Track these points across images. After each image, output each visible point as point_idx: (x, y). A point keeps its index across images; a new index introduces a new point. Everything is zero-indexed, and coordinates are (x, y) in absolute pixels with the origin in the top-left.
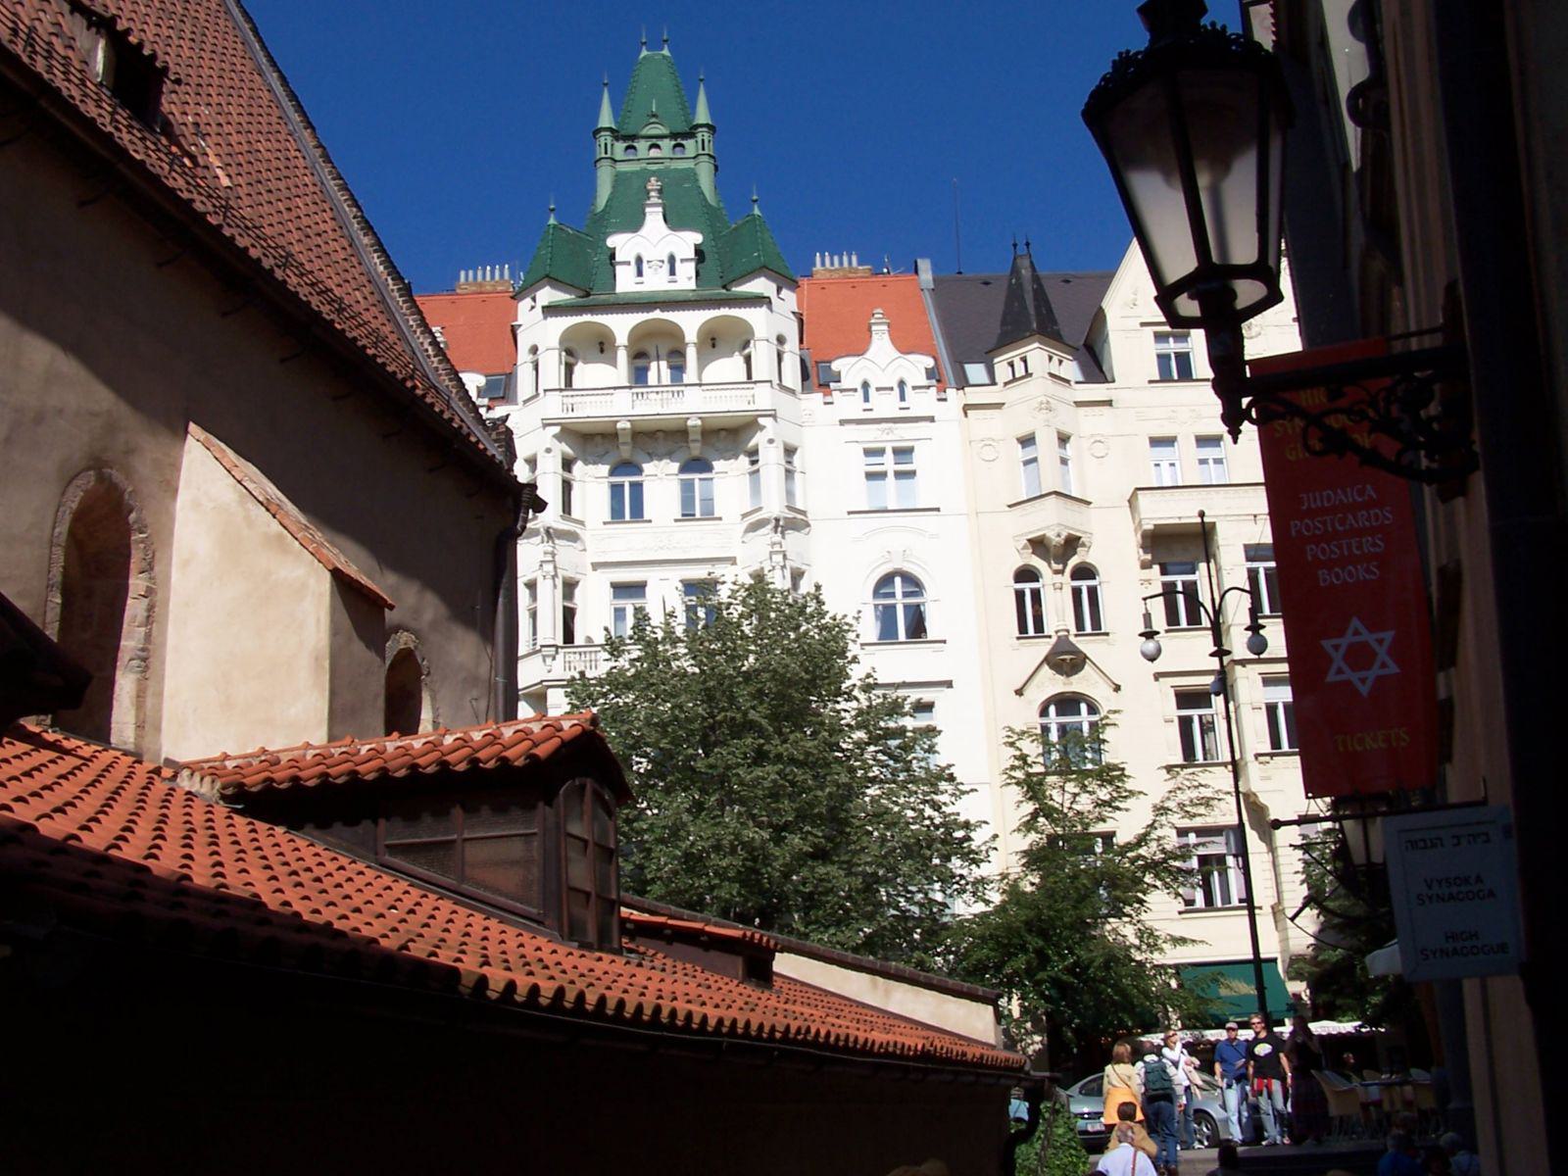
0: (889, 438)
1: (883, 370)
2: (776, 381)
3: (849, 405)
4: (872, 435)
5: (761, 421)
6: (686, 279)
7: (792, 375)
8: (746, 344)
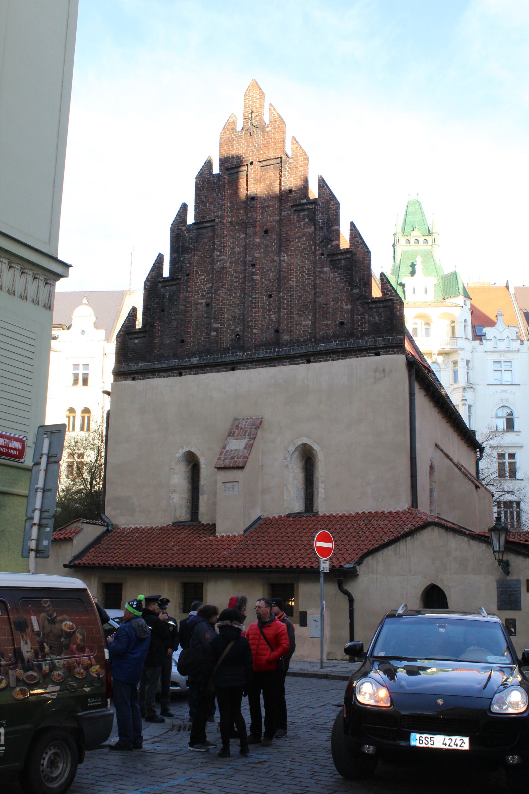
0: (502, 358)
1: (501, 333)
2: (464, 337)
3: (488, 345)
4: (496, 356)
5: (459, 352)
6: (431, 297)
7: (470, 335)
8: (453, 322)
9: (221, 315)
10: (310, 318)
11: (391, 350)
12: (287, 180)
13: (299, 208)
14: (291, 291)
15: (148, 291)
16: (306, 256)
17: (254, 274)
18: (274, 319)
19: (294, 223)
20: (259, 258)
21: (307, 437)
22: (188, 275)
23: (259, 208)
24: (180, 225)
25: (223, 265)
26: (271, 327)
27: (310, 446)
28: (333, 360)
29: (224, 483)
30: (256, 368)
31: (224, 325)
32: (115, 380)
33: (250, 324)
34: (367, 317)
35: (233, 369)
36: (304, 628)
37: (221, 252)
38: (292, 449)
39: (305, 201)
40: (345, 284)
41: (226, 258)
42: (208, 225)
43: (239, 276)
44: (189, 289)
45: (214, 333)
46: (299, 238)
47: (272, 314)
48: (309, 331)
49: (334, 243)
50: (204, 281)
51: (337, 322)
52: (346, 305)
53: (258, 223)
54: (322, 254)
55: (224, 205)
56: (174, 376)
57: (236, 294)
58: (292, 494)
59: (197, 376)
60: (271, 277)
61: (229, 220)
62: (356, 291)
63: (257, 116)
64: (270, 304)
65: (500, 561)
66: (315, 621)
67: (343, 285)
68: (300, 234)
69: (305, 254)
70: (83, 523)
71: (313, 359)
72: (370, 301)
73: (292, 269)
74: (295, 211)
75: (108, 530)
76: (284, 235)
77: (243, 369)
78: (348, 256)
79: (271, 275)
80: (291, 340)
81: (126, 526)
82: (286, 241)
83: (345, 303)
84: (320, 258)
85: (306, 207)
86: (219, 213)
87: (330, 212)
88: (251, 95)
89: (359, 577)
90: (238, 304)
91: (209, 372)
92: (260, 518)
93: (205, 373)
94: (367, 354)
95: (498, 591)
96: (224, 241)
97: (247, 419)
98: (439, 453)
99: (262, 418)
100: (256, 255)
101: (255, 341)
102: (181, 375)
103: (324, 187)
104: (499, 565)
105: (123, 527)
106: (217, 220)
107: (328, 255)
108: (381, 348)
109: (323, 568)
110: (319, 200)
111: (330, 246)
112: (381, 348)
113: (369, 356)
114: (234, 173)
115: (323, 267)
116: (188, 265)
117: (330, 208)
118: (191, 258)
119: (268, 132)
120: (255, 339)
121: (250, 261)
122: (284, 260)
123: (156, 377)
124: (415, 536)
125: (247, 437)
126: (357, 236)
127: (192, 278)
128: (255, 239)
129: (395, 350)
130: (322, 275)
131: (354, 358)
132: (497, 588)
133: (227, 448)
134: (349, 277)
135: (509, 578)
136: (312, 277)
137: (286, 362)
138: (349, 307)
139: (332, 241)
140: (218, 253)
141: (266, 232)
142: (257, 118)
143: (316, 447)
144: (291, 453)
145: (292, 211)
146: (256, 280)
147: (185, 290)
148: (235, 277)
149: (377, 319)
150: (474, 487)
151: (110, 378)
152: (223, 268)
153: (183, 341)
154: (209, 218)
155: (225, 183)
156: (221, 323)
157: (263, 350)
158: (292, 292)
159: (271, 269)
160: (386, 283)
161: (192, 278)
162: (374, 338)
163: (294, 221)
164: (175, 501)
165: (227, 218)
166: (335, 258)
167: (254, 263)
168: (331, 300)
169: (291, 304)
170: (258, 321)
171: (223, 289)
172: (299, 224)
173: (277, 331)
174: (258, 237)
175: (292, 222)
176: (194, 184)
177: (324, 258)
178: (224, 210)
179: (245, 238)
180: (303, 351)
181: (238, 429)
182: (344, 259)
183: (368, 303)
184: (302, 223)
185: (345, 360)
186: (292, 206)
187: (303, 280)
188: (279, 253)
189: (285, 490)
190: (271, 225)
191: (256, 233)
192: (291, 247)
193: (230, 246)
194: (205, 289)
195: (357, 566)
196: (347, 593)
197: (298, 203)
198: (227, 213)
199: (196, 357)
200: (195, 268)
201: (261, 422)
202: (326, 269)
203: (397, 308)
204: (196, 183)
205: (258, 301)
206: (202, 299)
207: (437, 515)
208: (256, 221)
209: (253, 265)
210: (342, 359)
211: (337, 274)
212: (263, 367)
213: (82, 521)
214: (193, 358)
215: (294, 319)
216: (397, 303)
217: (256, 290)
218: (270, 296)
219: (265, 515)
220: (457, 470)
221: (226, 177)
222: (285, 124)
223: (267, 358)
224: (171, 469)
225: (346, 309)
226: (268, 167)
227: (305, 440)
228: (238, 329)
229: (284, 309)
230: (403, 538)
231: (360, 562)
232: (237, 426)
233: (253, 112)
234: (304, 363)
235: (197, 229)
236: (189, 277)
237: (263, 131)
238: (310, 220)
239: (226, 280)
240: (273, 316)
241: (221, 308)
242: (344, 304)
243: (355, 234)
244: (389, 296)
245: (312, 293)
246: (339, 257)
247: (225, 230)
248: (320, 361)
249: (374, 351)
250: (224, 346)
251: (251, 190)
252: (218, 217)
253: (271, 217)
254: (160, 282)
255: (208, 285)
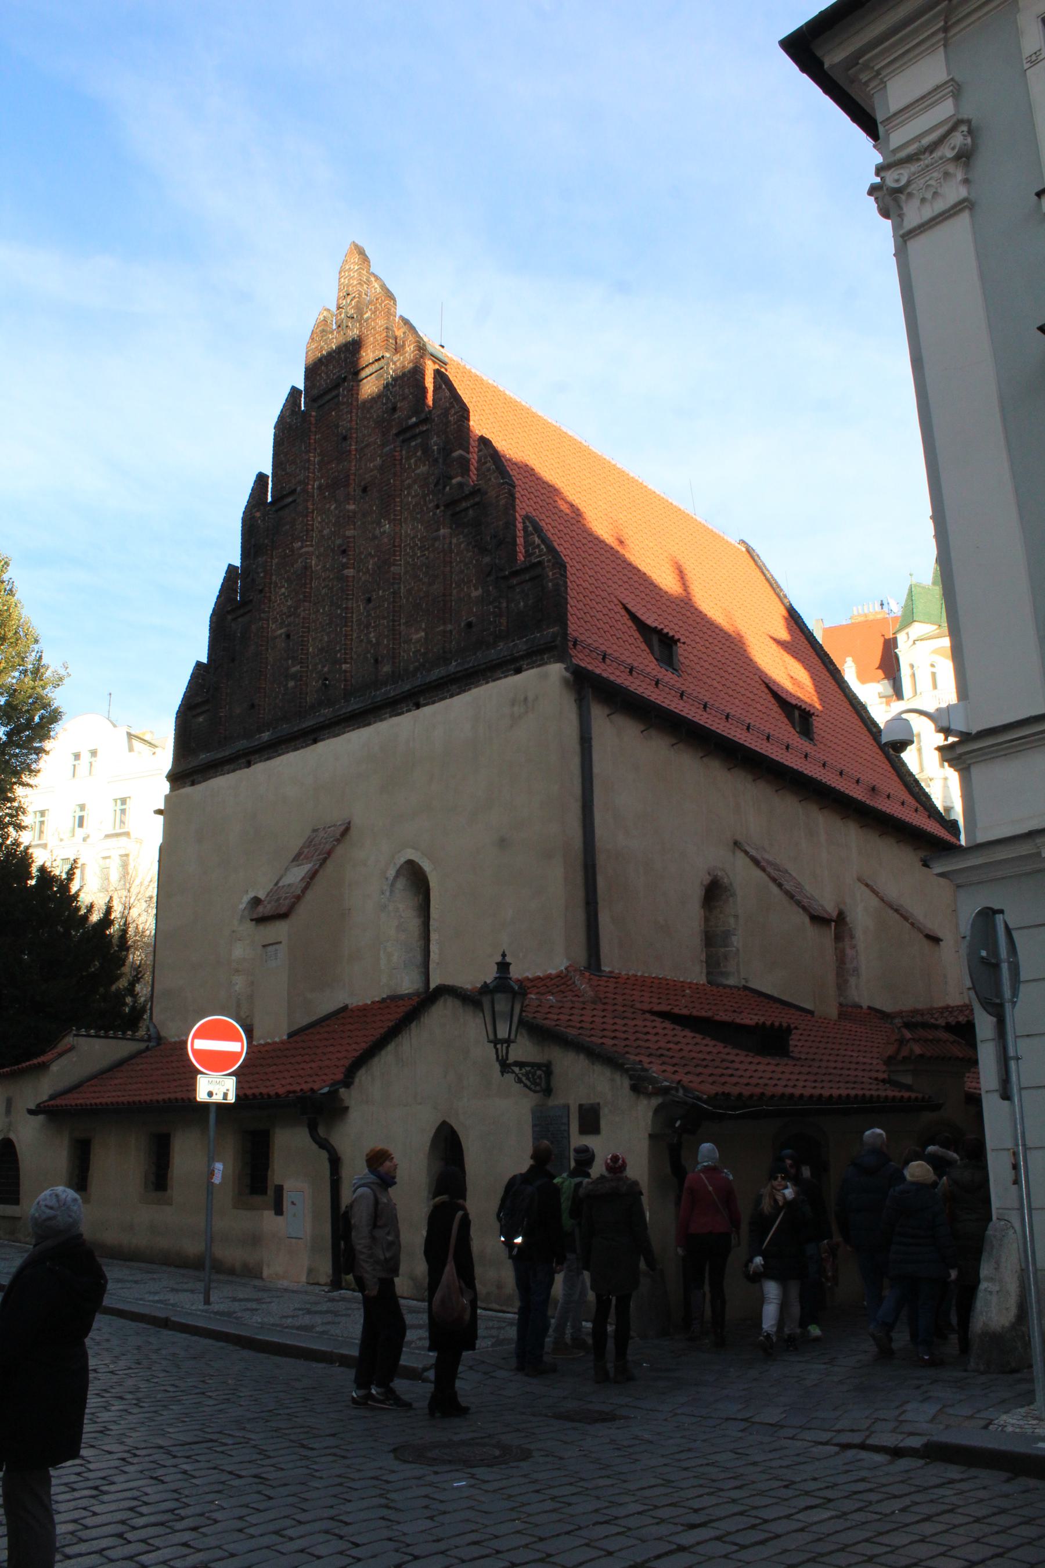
9: (302, 649)
10: (423, 626)
11: (539, 658)
12: (391, 393)
13: (408, 435)
14: (393, 584)
15: (214, 631)
16: (419, 516)
17: (345, 566)
18: (374, 640)
19: (401, 464)
20: (354, 537)
21: (414, 848)
22: (261, 591)
23: (354, 453)
24: (254, 511)
25: (306, 563)
26: (369, 655)
27: (418, 864)
28: (452, 696)
29: (264, 946)
30: (344, 733)
31: (308, 667)
32: (172, 789)
33: (339, 655)
34: (504, 605)
35: (315, 741)
36: (280, 1218)
37: (302, 541)
38: (391, 873)
39: (414, 420)
40: (474, 552)
41: (311, 549)
42: (290, 499)
43: (329, 577)
44: (262, 615)
45: (291, 684)
46: (409, 487)
47: (370, 633)
48: (422, 650)
49: (454, 481)
50: (285, 597)
51: (463, 624)
52: (476, 589)
53: (352, 477)
54: (437, 507)
55: (309, 460)
56: (240, 769)
57: (324, 609)
58: (395, 958)
59: (268, 762)
60: (370, 567)
61: (316, 484)
62: (487, 560)
63: (352, 300)
64: (369, 615)
65: (505, 1066)
66: (293, 1203)
67: (471, 554)
68: (409, 481)
69: (417, 513)
70: (75, 1035)
71: (424, 700)
72: (507, 573)
73: (397, 544)
74: (403, 441)
75: (147, 1049)
76: (385, 488)
77: (328, 738)
78: (477, 499)
79: (371, 562)
80: (393, 672)
81: (177, 1039)
82: (389, 497)
83: (474, 586)
84: (434, 514)
85: (417, 431)
86: (301, 477)
87: (448, 430)
88: (347, 267)
89: (351, 1110)
90: (327, 624)
91: (283, 754)
92: (345, 1008)
93: (279, 755)
94: (503, 673)
95: (534, 1132)
96: (308, 520)
97: (329, 827)
98: (741, 860)
99: (349, 823)
100: (349, 533)
101: (345, 685)
102: (249, 764)
103: (440, 387)
104: (502, 1073)
105: (173, 1040)
106: (299, 489)
107: (444, 506)
108: (522, 657)
109: (210, 1094)
110: (434, 412)
111: (448, 488)
112: (522, 657)
113: (506, 677)
114: (324, 404)
115: (438, 530)
116: (262, 575)
117: (450, 422)
118: (267, 562)
119: (367, 320)
120: (346, 680)
121: (340, 546)
122: (385, 532)
123: (221, 775)
124: (422, 1019)
125: (314, 858)
126: (489, 459)
127: (268, 595)
128: (347, 506)
129: (545, 657)
130: (437, 544)
131: (482, 685)
132: (534, 1126)
133: (281, 884)
134: (479, 537)
135: (551, 1102)
136: (426, 552)
137: (386, 713)
138: (480, 591)
139: (451, 478)
140: (300, 543)
141: (365, 490)
142: (353, 302)
143: (426, 866)
144: (390, 882)
145: (398, 443)
146: (347, 576)
147: (258, 617)
148: (324, 580)
149: (522, 604)
150: (807, 920)
151: (165, 787)
152: (306, 568)
153: (253, 706)
154: (289, 488)
155: (311, 424)
156: (301, 663)
157: (355, 698)
158: (396, 586)
159: (370, 554)
160: (533, 534)
161: (268, 595)
162: (513, 641)
163: (401, 460)
164: (237, 988)
165: (315, 481)
166: (458, 509)
167: (344, 548)
168: (454, 585)
169: (394, 607)
170: (351, 649)
171: (306, 604)
172: (410, 464)
173: (376, 661)
174: (351, 502)
175: (397, 462)
176: (272, 437)
177: (440, 512)
178: (309, 468)
179: (336, 508)
180: (407, 687)
181: (309, 847)
182: (472, 506)
183: (505, 578)
184: (412, 461)
185: (469, 692)
186: (397, 435)
187: (414, 560)
188: (379, 524)
189: (382, 952)
190: (371, 476)
191: (348, 494)
192: (395, 506)
193: (317, 528)
194: (285, 610)
195: (342, 1090)
196: (324, 1145)
197: (404, 426)
198: (314, 473)
199: (268, 731)
200: (274, 577)
201: (347, 830)
202: (442, 531)
203: (548, 576)
204: (275, 435)
205: (352, 613)
206: (281, 628)
207: (743, 982)
208: (349, 476)
209: (344, 552)
210: (464, 691)
211: (461, 536)
212: (354, 730)
213: (74, 1032)
214: (264, 732)
215: (400, 633)
216: (548, 567)
217: (348, 595)
218: (369, 600)
219: (354, 1002)
220: (775, 889)
221: (314, 414)
222: (394, 300)
223: (357, 711)
224: (233, 932)
225: (476, 597)
226: (369, 378)
227: (410, 854)
228: (326, 669)
229: (384, 618)
230: (407, 1026)
231: (348, 1080)
232: (311, 842)
233: (348, 295)
234: (409, 711)
235: (277, 511)
236: (262, 595)
237: (360, 321)
238: (423, 453)
239: (311, 588)
240: (372, 635)
241: (302, 636)
242: (472, 588)
243: (486, 458)
244: (537, 557)
245: (426, 580)
246: (464, 505)
247: (309, 504)
248: (434, 703)
249: (513, 667)
250: (306, 702)
251: (342, 426)
252: (300, 482)
253: (370, 463)
254: (228, 612)
255: (289, 603)
